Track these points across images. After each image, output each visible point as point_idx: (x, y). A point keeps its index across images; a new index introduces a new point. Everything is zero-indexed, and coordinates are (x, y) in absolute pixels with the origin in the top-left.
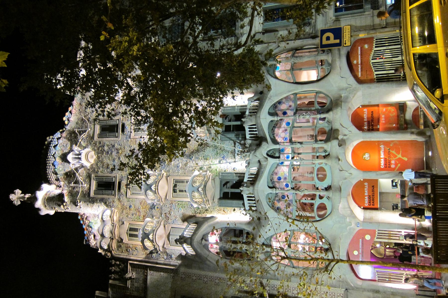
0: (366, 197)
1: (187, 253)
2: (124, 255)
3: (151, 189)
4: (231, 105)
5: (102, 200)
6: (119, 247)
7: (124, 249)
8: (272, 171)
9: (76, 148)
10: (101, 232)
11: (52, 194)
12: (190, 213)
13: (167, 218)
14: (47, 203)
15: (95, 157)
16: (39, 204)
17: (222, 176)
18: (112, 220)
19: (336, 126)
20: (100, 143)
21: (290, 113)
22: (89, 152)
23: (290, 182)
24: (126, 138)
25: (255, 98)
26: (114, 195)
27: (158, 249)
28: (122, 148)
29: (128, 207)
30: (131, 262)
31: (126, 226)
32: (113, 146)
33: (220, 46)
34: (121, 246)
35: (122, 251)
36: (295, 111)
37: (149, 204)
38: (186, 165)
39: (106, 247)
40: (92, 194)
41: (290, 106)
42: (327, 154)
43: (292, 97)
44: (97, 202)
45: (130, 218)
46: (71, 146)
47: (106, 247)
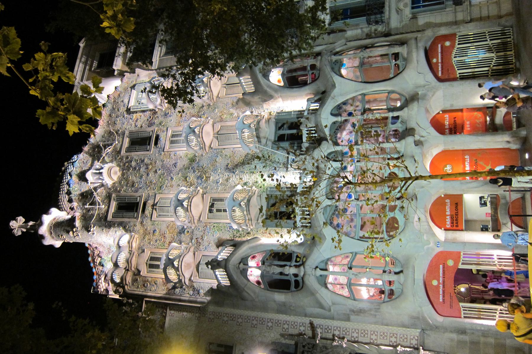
0: (448, 217)
1: (219, 284)
2: (140, 291)
3: (182, 205)
4: (287, 111)
5: (120, 224)
6: (135, 281)
7: (141, 283)
9: (97, 164)
10: (114, 260)
11: (61, 219)
12: (227, 236)
13: (198, 244)
14: (54, 229)
15: (119, 174)
16: (43, 230)
17: (270, 191)
19: (412, 124)
20: (127, 158)
22: (113, 167)
24: (159, 151)
25: (316, 99)
26: (137, 218)
27: (183, 281)
28: (153, 163)
29: (152, 231)
31: (147, 255)
32: (143, 161)
34: (137, 280)
37: (178, 226)
38: (227, 180)
39: (118, 280)
40: (110, 217)
43: (360, 97)
44: (114, 227)
47: (118, 280)
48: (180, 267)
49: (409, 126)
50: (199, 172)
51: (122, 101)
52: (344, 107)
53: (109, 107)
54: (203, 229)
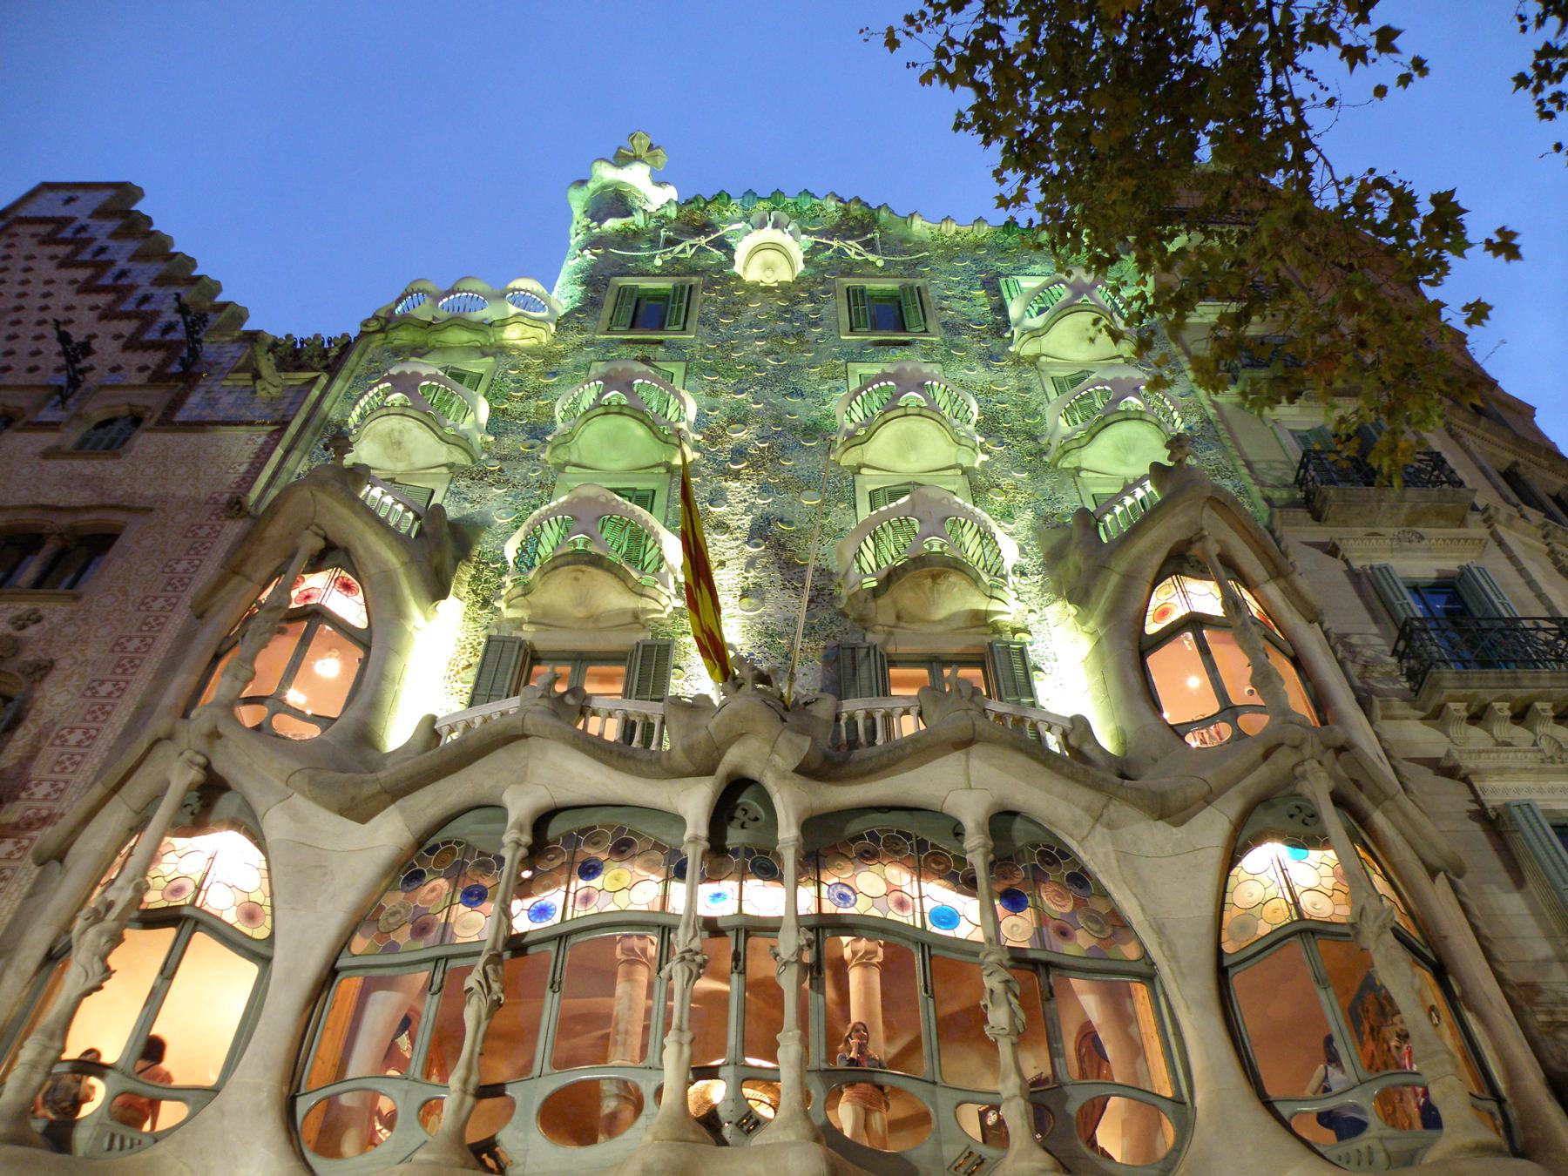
8: (642, 827)
13: (478, 475)
15: (769, 280)
18: (504, 323)
21: (1018, 929)
25: (1087, 749)
26: (609, 331)
29: (554, 369)
30: (324, 379)
31: (477, 365)
32: (815, 324)
33: (1346, 635)
35: (371, 361)
36: (1032, 955)
42: (728, 1129)
45: (506, 374)
48: (384, 411)
50: (762, 450)
51: (1032, 262)
53: (1010, 240)
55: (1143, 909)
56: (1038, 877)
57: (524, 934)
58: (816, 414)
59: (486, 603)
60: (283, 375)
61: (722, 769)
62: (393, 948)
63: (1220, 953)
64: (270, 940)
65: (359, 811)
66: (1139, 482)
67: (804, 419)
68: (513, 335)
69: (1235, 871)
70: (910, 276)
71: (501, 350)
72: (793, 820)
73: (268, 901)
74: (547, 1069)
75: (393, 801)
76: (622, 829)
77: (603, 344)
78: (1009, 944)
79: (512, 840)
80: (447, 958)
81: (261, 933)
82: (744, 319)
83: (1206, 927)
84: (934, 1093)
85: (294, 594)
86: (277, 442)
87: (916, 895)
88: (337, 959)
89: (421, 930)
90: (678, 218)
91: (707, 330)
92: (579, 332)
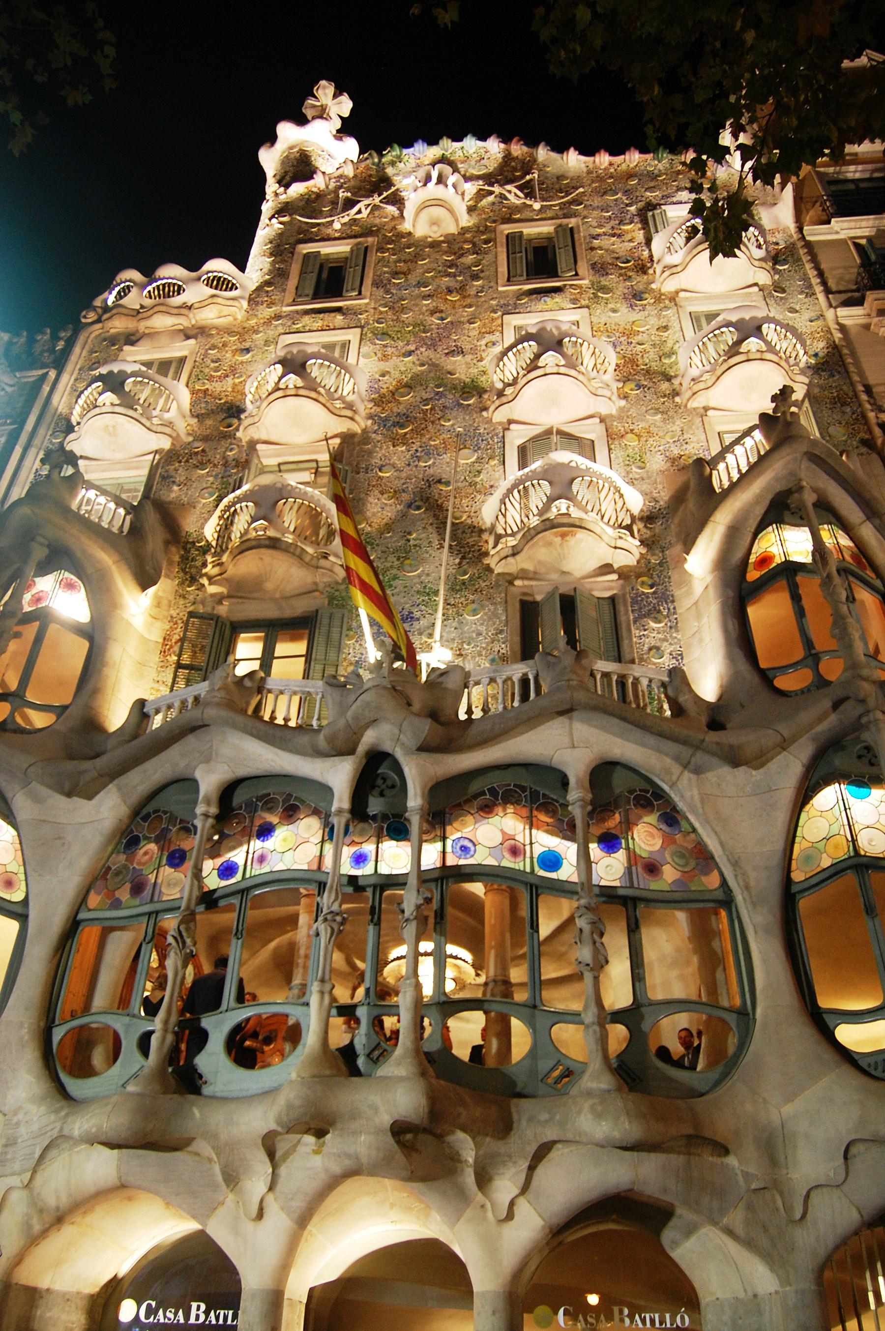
2: (78, 355)
6: (113, 340)
15: (436, 234)
18: (203, 305)
20: (486, 242)
22: (451, 211)
23: (243, 885)
25: (681, 699)
26: (294, 303)
28: (468, 301)
29: (247, 345)
30: (52, 374)
32: (475, 277)
34: (114, 345)
36: (622, 892)
41: (653, 868)
42: (361, 1062)
43: (712, 881)
45: (206, 355)
46: (478, 178)
49: (522, 1109)
50: (425, 412)
52: (652, 818)
54: (230, 459)
55: (722, 844)
56: (628, 825)
57: (215, 891)
58: (474, 371)
59: (193, 580)
60: (18, 375)
61: (362, 749)
62: (116, 904)
63: (787, 881)
64: (25, 902)
65: (85, 790)
66: (748, 433)
67: (463, 377)
68: (209, 316)
69: (807, 807)
70: (566, 216)
71: (199, 332)
72: (419, 791)
73: (22, 869)
74: (233, 1004)
75: (111, 782)
76: (290, 795)
77: (289, 316)
78: (603, 883)
79: (204, 810)
80: (157, 913)
81: (17, 896)
82: (413, 278)
83: (776, 860)
84: (533, 1016)
85: (27, 597)
86: (15, 444)
87: (527, 842)
88: (77, 913)
89: (137, 888)
90: (355, 176)
91: (381, 292)
92: (269, 307)
